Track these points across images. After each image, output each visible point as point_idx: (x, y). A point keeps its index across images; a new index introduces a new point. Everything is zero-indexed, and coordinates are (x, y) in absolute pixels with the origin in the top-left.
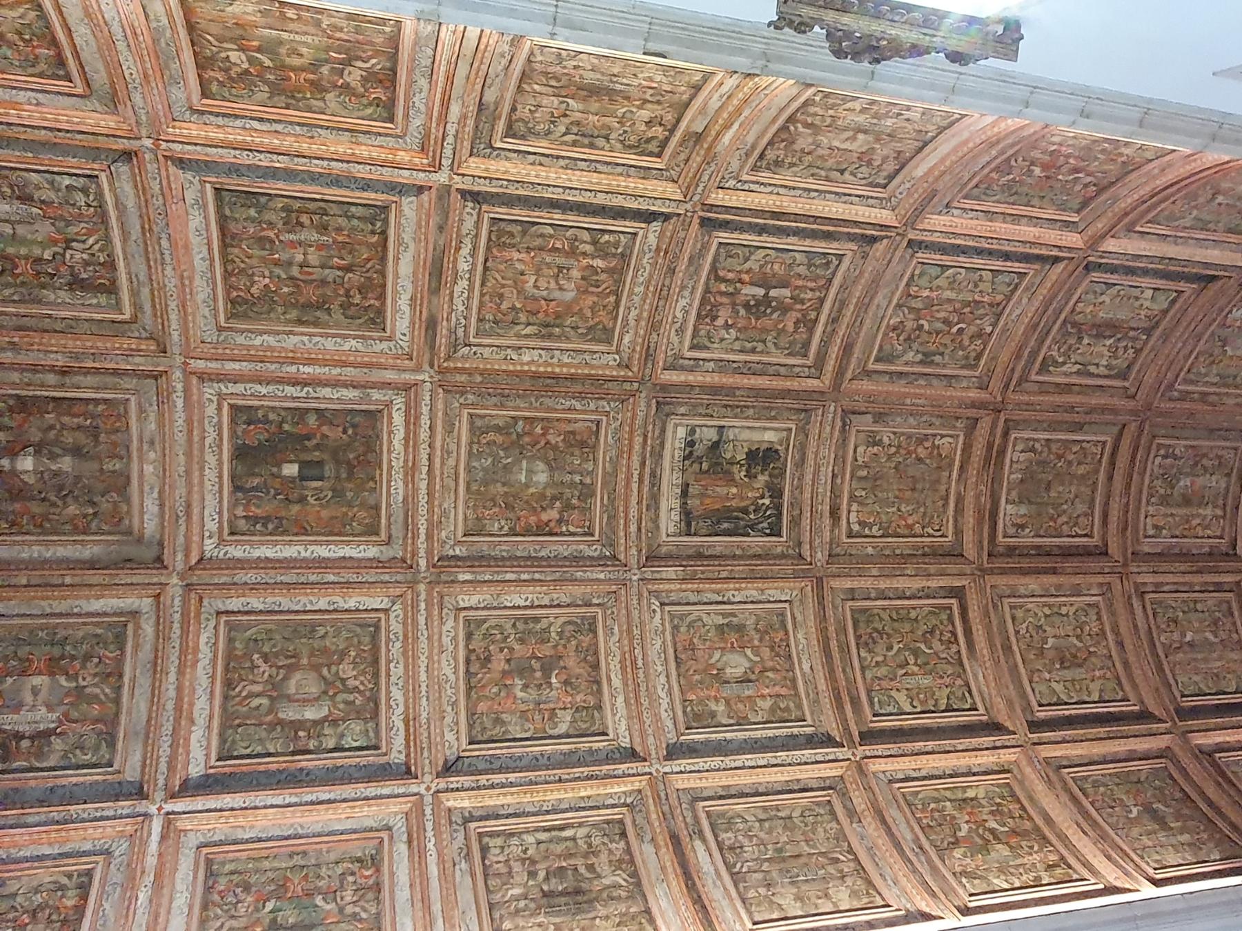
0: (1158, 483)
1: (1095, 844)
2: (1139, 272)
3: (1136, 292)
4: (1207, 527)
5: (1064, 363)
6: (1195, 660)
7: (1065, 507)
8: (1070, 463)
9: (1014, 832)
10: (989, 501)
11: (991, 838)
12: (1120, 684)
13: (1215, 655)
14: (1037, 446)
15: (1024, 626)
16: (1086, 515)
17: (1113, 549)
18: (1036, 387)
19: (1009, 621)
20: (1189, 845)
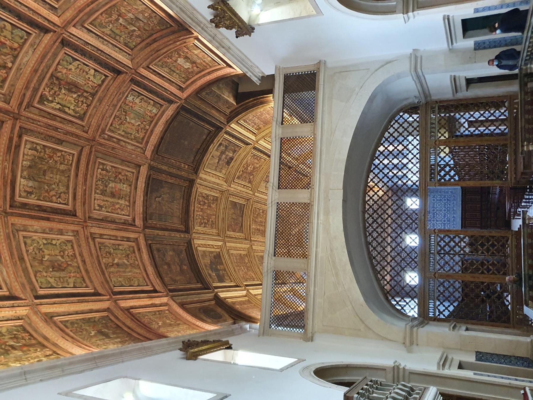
0: (100, 183)
1: (73, 343)
2: (87, 55)
3: (87, 69)
4: (122, 210)
5: (52, 102)
6: (120, 271)
7: (54, 186)
8: (56, 162)
9: (25, 345)
10: (10, 174)
11: (10, 349)
12: (84, 280)
13: (128, 270)
14: (38, 147)
15: (31, 248)
16: (65, 193)
17: (79, 213)
18: (37, 111)
19: (23, 245)
20: (120, 342)
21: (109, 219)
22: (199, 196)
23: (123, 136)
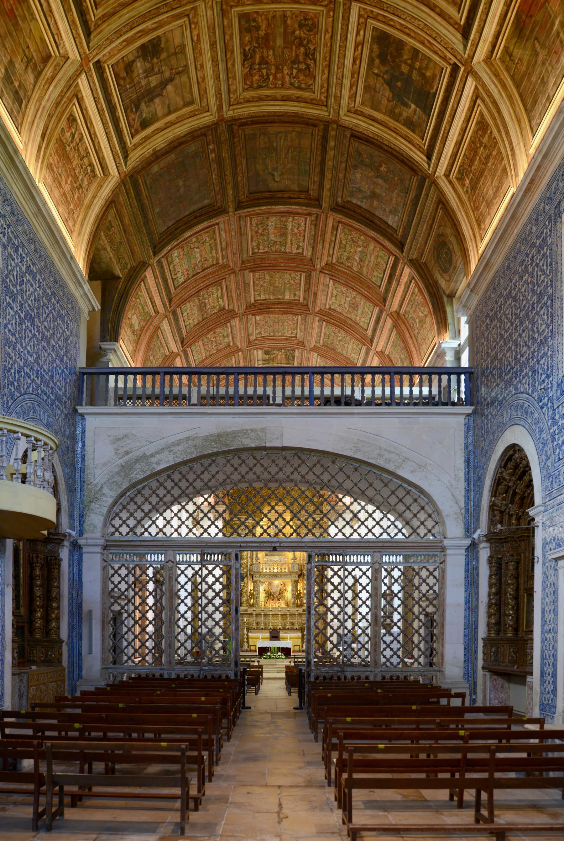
4: (299, 225)
21: (312, 241)
22: (251, 87)
23: (217, 250)
